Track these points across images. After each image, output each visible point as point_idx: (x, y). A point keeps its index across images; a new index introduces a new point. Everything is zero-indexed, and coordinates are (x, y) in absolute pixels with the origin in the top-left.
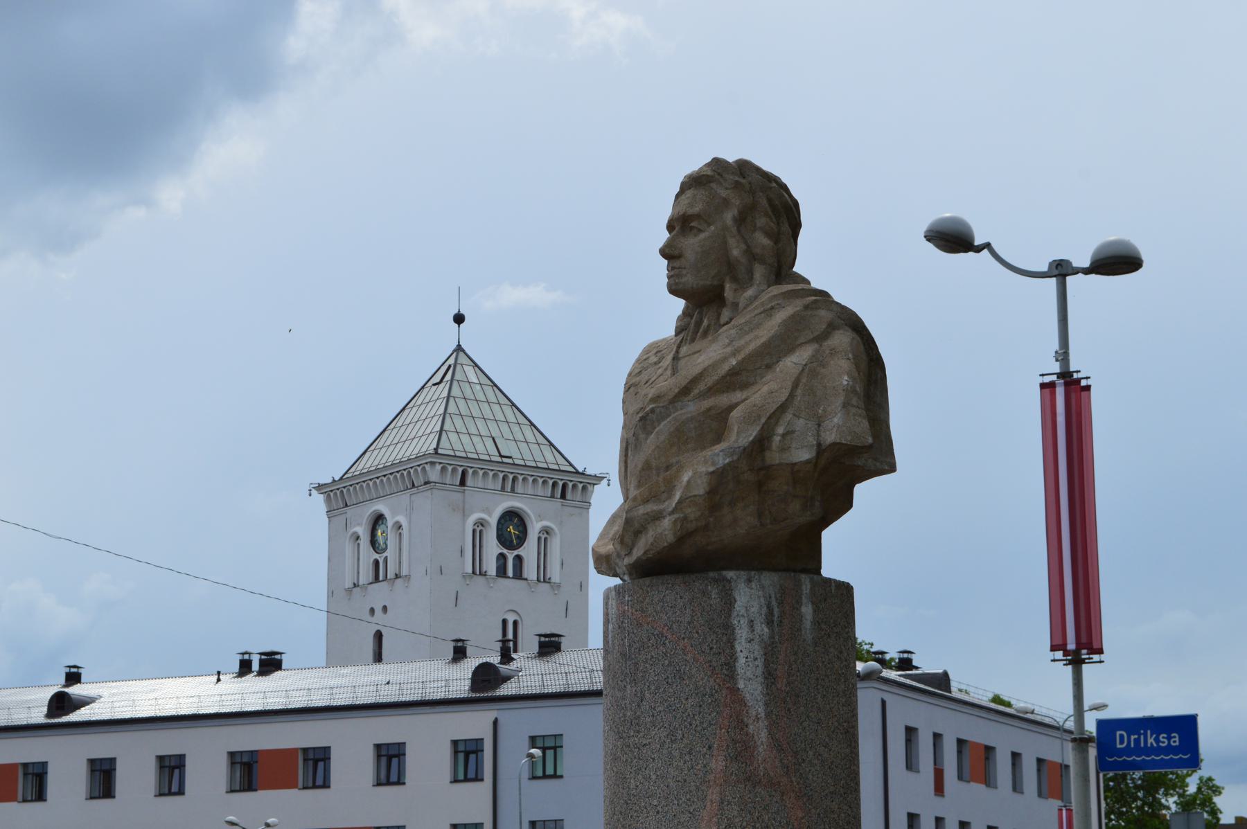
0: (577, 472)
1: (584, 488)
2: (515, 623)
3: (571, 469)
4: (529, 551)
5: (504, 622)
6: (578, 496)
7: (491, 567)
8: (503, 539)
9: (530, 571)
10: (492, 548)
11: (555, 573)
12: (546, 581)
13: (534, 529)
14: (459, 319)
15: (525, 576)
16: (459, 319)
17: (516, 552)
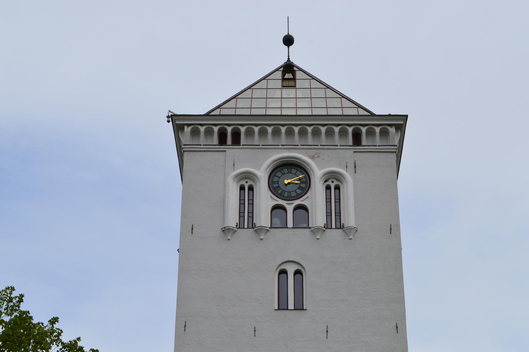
0: (372, 115)
1: (384, 133)
2: (298, 273)
3: (369, 114)
4: (316, 199)
5: (283, 272)
6: (378, 140)
7: (263, 218)
8: (275, 188)
9: (318, 217)
10: (264, 200)
11: (349, 218)
12: (341, 227)
13: (318, 173)
14: (288, 41)
15: (310, 226)
16: (288, 41)
17: (297, 202)
